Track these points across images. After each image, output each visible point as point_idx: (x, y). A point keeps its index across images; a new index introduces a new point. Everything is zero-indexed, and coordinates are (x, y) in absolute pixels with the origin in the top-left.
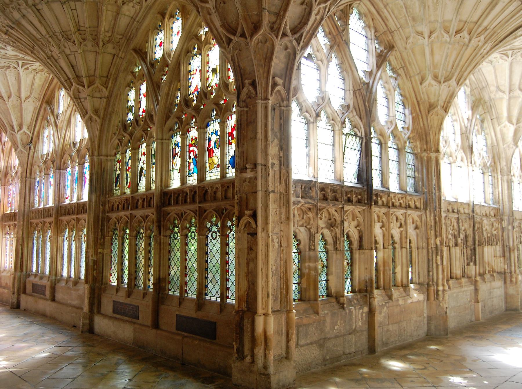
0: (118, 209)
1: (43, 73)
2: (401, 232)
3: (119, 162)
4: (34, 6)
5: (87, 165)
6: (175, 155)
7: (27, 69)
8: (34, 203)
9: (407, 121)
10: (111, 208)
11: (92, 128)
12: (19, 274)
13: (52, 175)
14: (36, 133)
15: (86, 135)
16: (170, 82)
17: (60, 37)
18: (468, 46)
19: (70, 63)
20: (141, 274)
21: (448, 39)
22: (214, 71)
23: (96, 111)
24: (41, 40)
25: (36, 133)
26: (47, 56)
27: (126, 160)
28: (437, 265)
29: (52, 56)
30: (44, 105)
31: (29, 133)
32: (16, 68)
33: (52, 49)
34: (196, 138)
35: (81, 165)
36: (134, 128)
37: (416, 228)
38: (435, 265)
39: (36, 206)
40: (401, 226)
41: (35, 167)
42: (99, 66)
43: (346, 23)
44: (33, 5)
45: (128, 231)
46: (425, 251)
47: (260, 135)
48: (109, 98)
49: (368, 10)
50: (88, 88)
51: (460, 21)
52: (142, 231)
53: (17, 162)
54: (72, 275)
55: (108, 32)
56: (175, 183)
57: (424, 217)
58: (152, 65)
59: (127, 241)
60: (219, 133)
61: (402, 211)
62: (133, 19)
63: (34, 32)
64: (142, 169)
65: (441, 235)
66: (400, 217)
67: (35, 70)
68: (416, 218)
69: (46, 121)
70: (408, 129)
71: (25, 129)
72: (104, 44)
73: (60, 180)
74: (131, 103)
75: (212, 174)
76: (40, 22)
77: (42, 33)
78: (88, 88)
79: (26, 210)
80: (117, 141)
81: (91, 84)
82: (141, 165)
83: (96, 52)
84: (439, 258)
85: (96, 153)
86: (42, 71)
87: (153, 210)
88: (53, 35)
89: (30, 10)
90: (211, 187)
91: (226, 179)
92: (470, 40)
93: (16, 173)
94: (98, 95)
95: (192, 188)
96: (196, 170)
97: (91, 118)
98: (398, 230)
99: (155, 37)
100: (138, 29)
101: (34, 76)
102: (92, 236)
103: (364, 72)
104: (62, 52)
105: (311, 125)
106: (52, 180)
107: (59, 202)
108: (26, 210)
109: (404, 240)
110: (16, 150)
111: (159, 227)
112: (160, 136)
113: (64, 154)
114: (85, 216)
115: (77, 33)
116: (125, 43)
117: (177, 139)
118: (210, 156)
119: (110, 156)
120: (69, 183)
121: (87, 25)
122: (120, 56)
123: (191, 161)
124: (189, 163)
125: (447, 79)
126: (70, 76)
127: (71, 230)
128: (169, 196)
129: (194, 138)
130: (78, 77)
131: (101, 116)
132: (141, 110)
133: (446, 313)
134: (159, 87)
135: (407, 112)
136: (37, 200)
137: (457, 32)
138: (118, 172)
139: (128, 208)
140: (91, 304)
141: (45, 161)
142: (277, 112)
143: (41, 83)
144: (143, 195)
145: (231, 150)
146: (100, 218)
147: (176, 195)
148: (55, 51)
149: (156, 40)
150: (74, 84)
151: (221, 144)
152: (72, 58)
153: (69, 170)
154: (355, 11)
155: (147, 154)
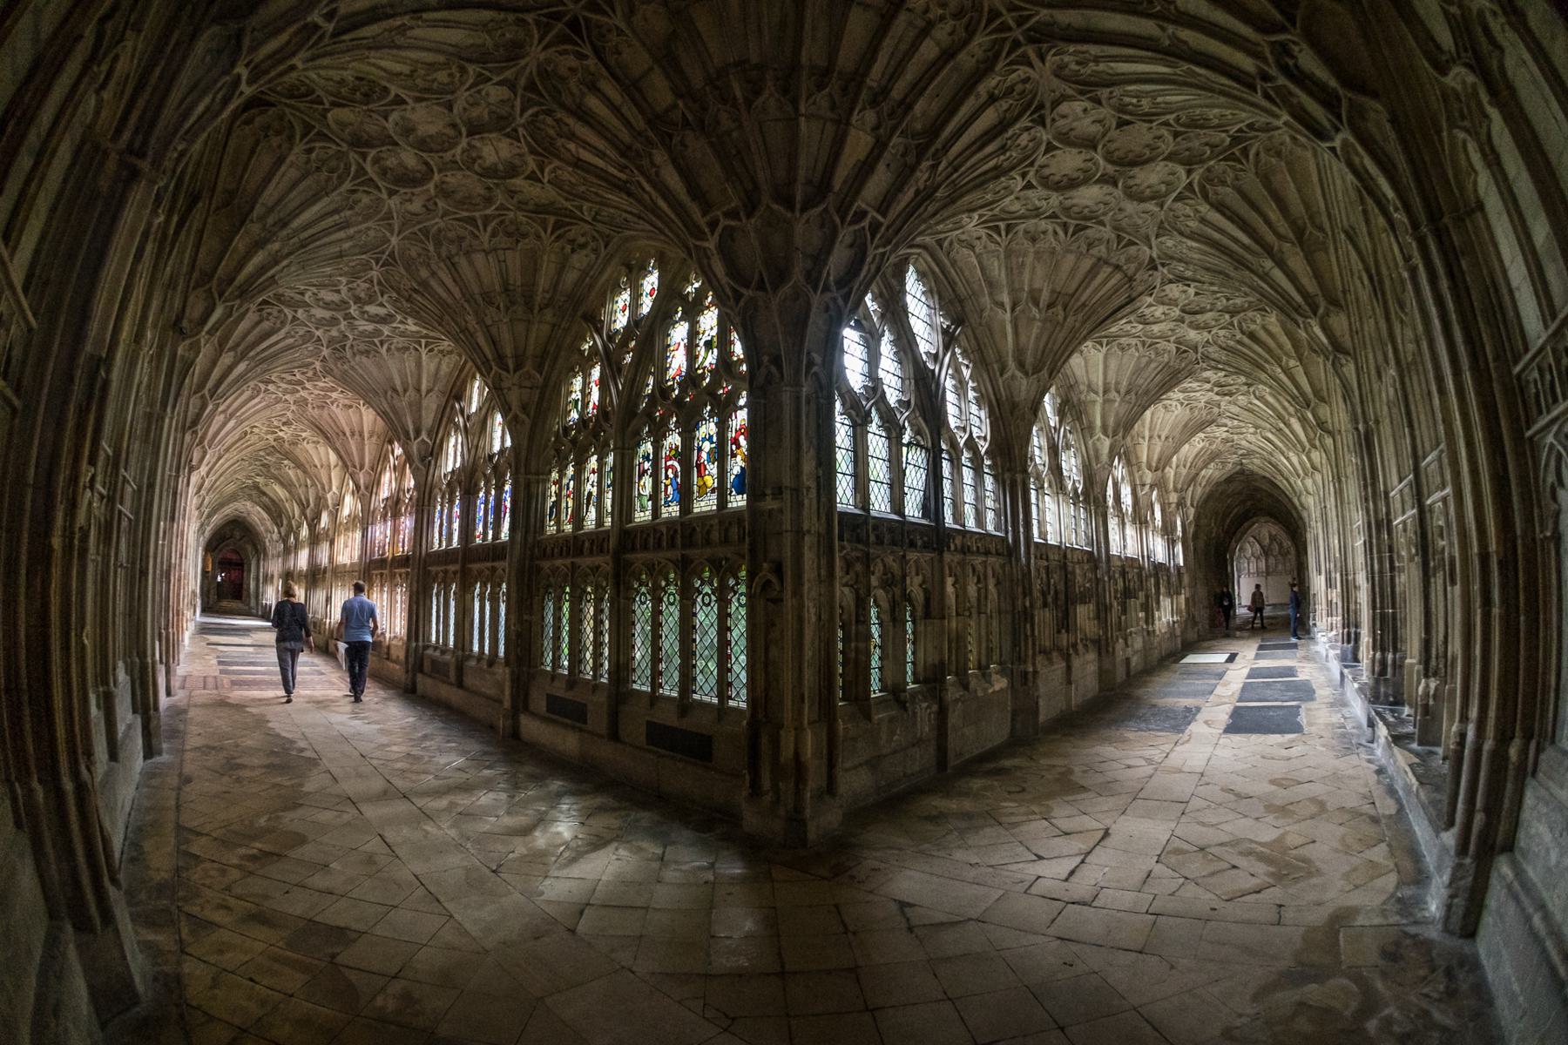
2: (979, 590)
3: (555, 483)
6: (642, 473)
9: (983, 428)
15: (508, 443)
16: (637, 362)
17: (479, 299)
18: (1063, 326)
20: (588, 655)
21: (1038, 316)
22: (708, 345)
23: (524, 408)
27: (565, 481)
28: (1026, 636)
33: (469, 318)
34: (677, 447)
36: (578, 432)
37: (998, 584)
38: (1022, 637)
40: (979, 581)
42: (532, 341)
43: (903, 283)
45: (568, 590)
46: (1009, 617)
47: (787, 442)
49: (929, 267)
50: (515, 371)
51: (1053, 291)
52: (589, 589)
54: (487, 651)
56: (642, 516)
57: (1007, 568)
58: (611, 338)
59: (567, 604)
60: (715, 439)
61: (981, 559)
62: (584, 273)
63: (444, 295)
64: (590, 494)
65: (1031, 594)
66: (979, 568)
68: (997, 567)
70: (985, 439)
72: (541, 309)
74: (577, 395)
75: (703, 504)
76: (454, 281)
78: (515, 371)
80: (553, 452)
81: (518, 367)
82: (588, 487)
83: (529, 321)
84: (1028, 626)
85: (522, 470)
87: (608, 558)
88: (468, 296)
89: (442, 265)
92: (1065, 318)
94: (527, 383)
95: (670, 522)
96: (677, 496)
97: (516, 418)
98: (975, 588)
100: (591, 286)
102: (514, 595)
103: (927, 353)
104: (481, 322)
105: (858, 429)
109: (983, 602)
111: (617, 585)
112: (620, 444)
114: (505, 564)
117: (647, 447)
118: (700, 475)
121: (519, 283)
123: (668, 482)
124: (666, 486)
125: (1037, 370)
126: (490, 357)
127: (484, 585)
130: (500, 358)
131: (532, 413)
132: (591, 405)
133: (1037, 703)
134: (619, 370)
135: (983, 414)
137: (1050, 306)
138: (554, 499)
139: (568, 554)
140: (514, 697)
142: (813, 406)
144: (590, 533)
145: (736, 466)
150: (495, 368)
151: (720, 455)
152: (494, 330)
154: (911, 268)
155: (600, 471)
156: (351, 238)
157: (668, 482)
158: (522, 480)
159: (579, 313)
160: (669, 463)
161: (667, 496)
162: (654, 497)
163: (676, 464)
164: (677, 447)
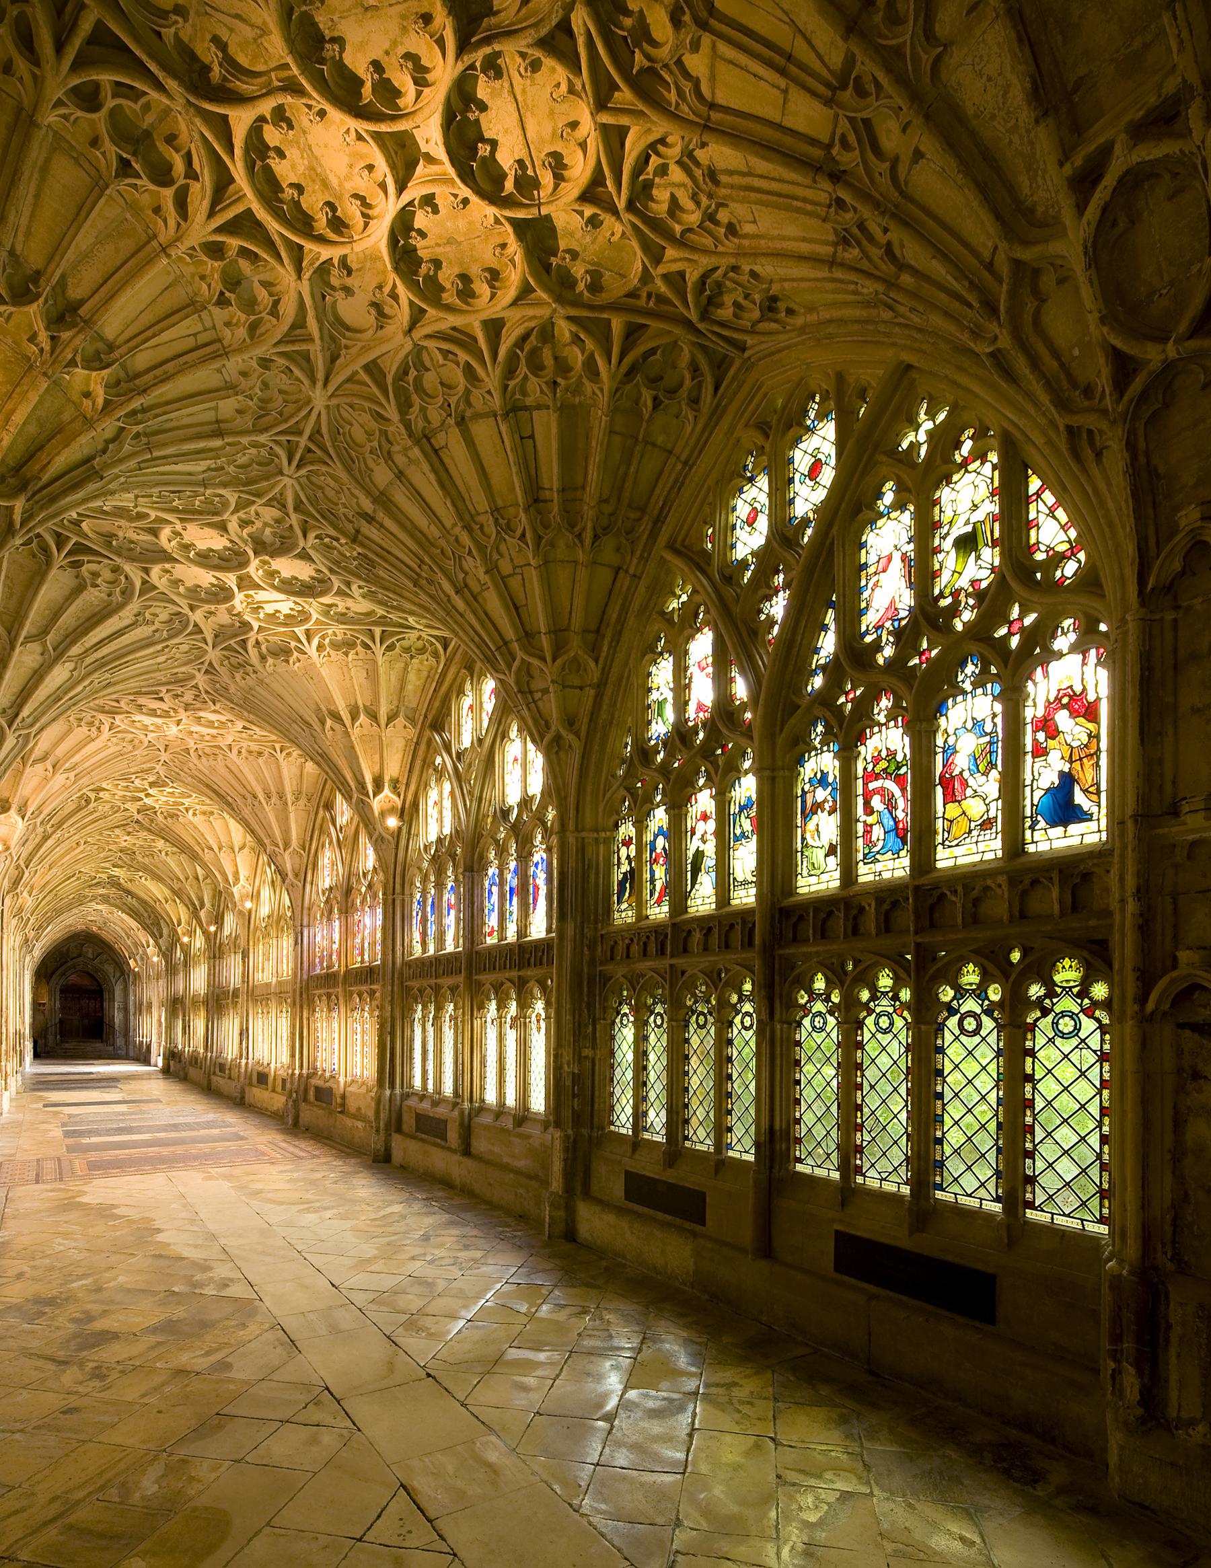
0: (628, 957)
1: (425, 656)
4: (428, 439)
7: (391, 648)
8: (411, 947)
10: (609, 953)
11: (559, 764)
17: (492, 530)
19: (512, 599)
24: (442, 543)
26: (455, 586)
29: (466, 586)
30: (427, 733)
32: (367, 647)
39: (418, 951)
44: (425, 436)
48: (601, 686)
55: (607, 501)
63: (422, 521)
67: (407, 650)
72: (596, 537)
77: (444, 520)
86: (422, 651)
90: (965, 886)
91: (1023, 860)
99: (732, 503)
101: (407, 665)
107: (473, 942)
115: (532, 509)
116: (647, 532)
117: (825, 762)
119: (604, 830)
122: (631, 571)
123: (871, 820)
126: (510, 634)
128: (794, 919)
129: (884, 754)
143: (420, 683)
146: (585, 977)
147: (822, 915)
148: (476, 568)
149: (734, 509)
152: (515, 583)
156: (230, 388)
157: (871, 820)
158: (571, 840)
159: (663, 539)
160: (872, 786)
161: (869, 843)
162: (845, 850)
163: (890, 785)
164: (892, 754)
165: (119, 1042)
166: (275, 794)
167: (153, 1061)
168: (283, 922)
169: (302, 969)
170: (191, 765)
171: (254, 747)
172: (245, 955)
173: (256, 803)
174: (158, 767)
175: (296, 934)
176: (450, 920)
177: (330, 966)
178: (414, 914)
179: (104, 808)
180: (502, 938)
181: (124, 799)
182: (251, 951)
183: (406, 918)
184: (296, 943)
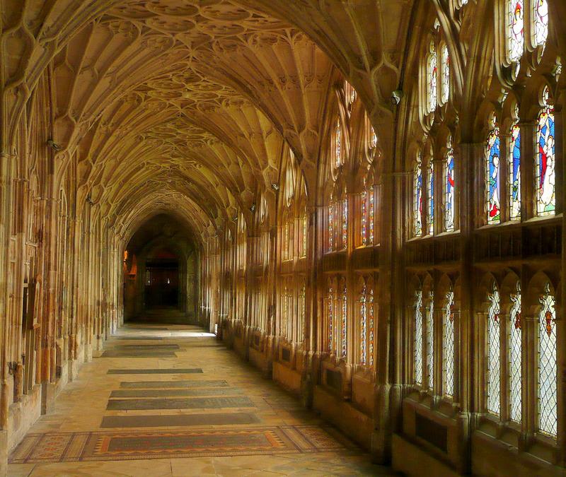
5: (546, 120)
8: (413, 228)
12: (388, 387)
13: (450, 159)
14: (409, 66)
25: (409, 66)
31: (396, 69)
35: (529, 123)
41: (414, 145)
53: (375, 140)
69: (429, 35)
71: (385, 60)
73: (472, 169)
79: (399, 243)
93: (374, 164)
106: (449, 172)
107: (472, 223)
108: (399, 243)
110: (369, 113)
113: (481, 100)
120: (493, 173)
136: (419, 219)
141: (432, 128)
153: (493, 140)
165: (190, 308)
166: (288, 78)
167: (211, 328)
168: (303, 203)
169: (316, 250)
170: (215, 58)
171: (266, 33)
172: (273, 234)
173: (272, 89)
174: (190, 64)
175: (311, 214)
176: (450, 196)
177: (341, 246)
178: (416, 192)
179: (153, 106)
180: (505, 216)
181: (168, 97)
182: (279, 230)
183: (407, 195)
184: (311, 224)
